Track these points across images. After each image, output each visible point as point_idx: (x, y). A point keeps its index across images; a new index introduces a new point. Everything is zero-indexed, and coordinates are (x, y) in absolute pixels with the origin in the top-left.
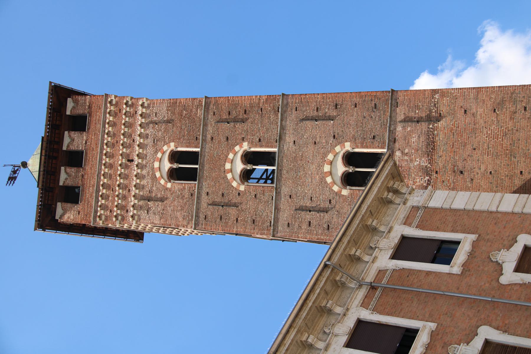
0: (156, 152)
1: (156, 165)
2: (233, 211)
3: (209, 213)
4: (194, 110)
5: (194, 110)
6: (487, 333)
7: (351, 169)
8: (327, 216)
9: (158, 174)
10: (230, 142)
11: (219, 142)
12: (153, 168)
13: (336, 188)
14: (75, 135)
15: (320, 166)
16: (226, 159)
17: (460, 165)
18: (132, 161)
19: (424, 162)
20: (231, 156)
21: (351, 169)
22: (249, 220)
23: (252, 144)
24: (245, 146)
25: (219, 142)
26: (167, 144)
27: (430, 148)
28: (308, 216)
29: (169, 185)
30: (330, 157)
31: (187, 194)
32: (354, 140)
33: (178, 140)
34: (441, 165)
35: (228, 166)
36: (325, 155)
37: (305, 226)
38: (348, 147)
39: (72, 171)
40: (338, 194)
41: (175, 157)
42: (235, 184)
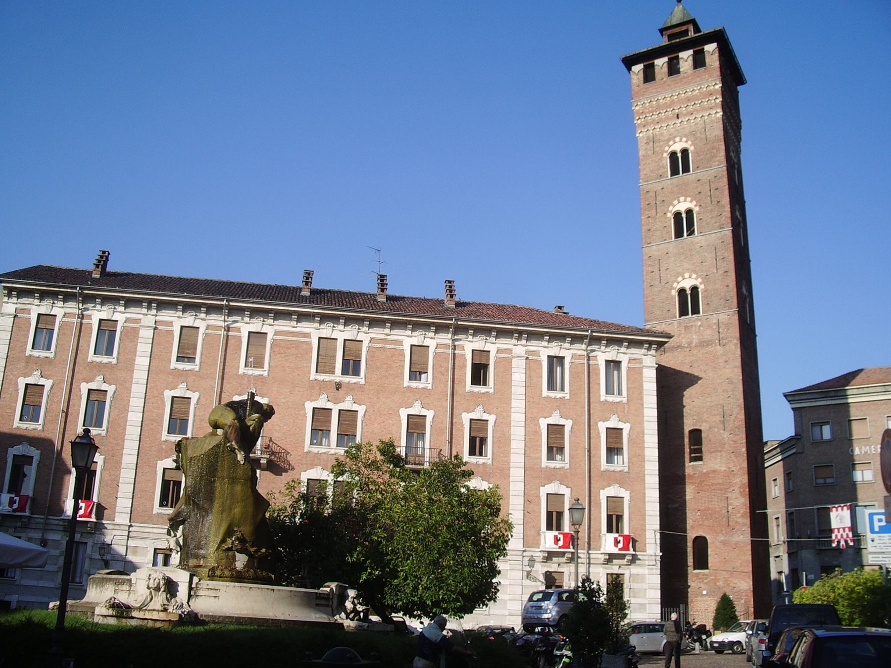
0: (686, 136)
1: (677, 139)
2: (653, 212)
3: (651, 194)
4: (718, 159)
5: (718, 159)
6: (568, 424)
7: (689, 292)
8: (657, 283)
9: (671, 143)
10: (697, 196)
11: (697, 187)
12: (675, 137)
13: (675, 285)
14: (690, 61)
15: (688, 270)
16: (686, 196)
17: (696, 365)
18: (678, 117)
19: (695, 342)
20: (689, 199)
21: (689, 292)
22: (649, 227)
23: (698, 213)
24: (696, 210)
25: (697, 187)
26: (692, 144)
27: (703, 344)
28: (656, 270)
29: (665, 155)
30: (694, 276)
31: (660, 172)
32: (705, 291)
33: (696, 152)
34: (695, 352)
35: (682, 199)
36: (695, 272)
37: (650, 269)
38: (701, 288)
39: (665, 69)
40: (672, 288)
41: (685, 152)
42: (671, 208)
